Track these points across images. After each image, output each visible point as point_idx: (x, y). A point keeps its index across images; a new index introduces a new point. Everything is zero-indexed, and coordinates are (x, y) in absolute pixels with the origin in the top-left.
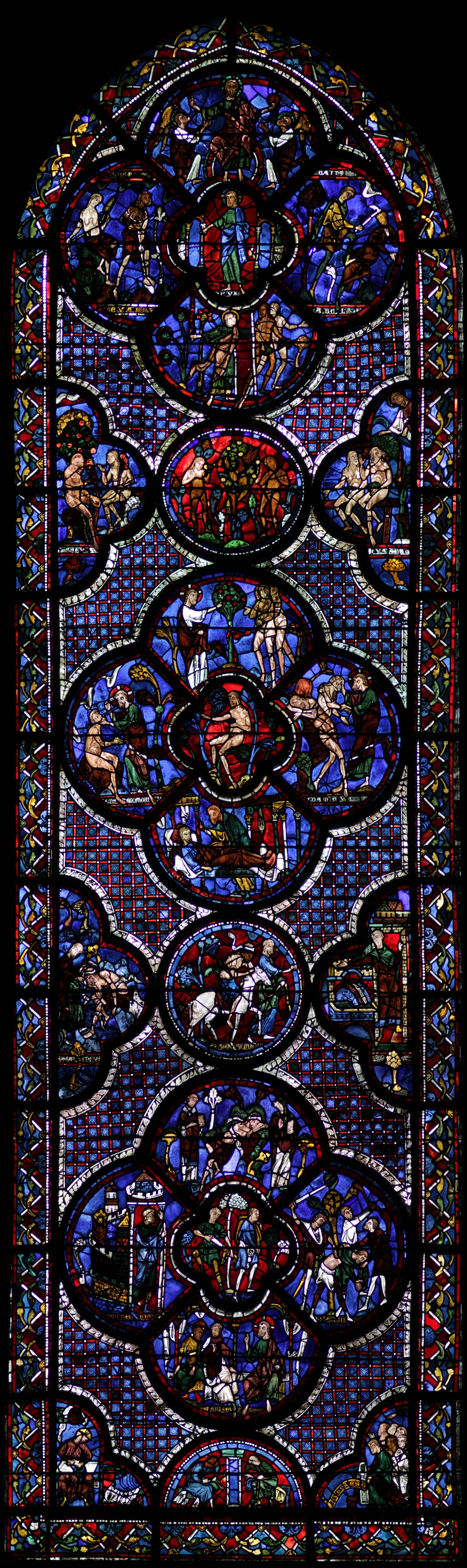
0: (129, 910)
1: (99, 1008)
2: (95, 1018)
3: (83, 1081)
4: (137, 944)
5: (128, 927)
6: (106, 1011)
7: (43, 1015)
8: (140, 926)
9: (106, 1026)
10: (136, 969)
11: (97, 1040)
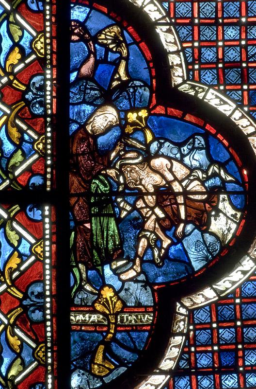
0: (212, 44)
1: (150, 224)
2: (143, 243)
3: (117, 358)
4: (227, 108)
5: (208, 77)
6: (164, 230)
7: (40, 238)
8: (233, 75)
9: (165, 257)
10: (224, 155)
11: (148, 283)
